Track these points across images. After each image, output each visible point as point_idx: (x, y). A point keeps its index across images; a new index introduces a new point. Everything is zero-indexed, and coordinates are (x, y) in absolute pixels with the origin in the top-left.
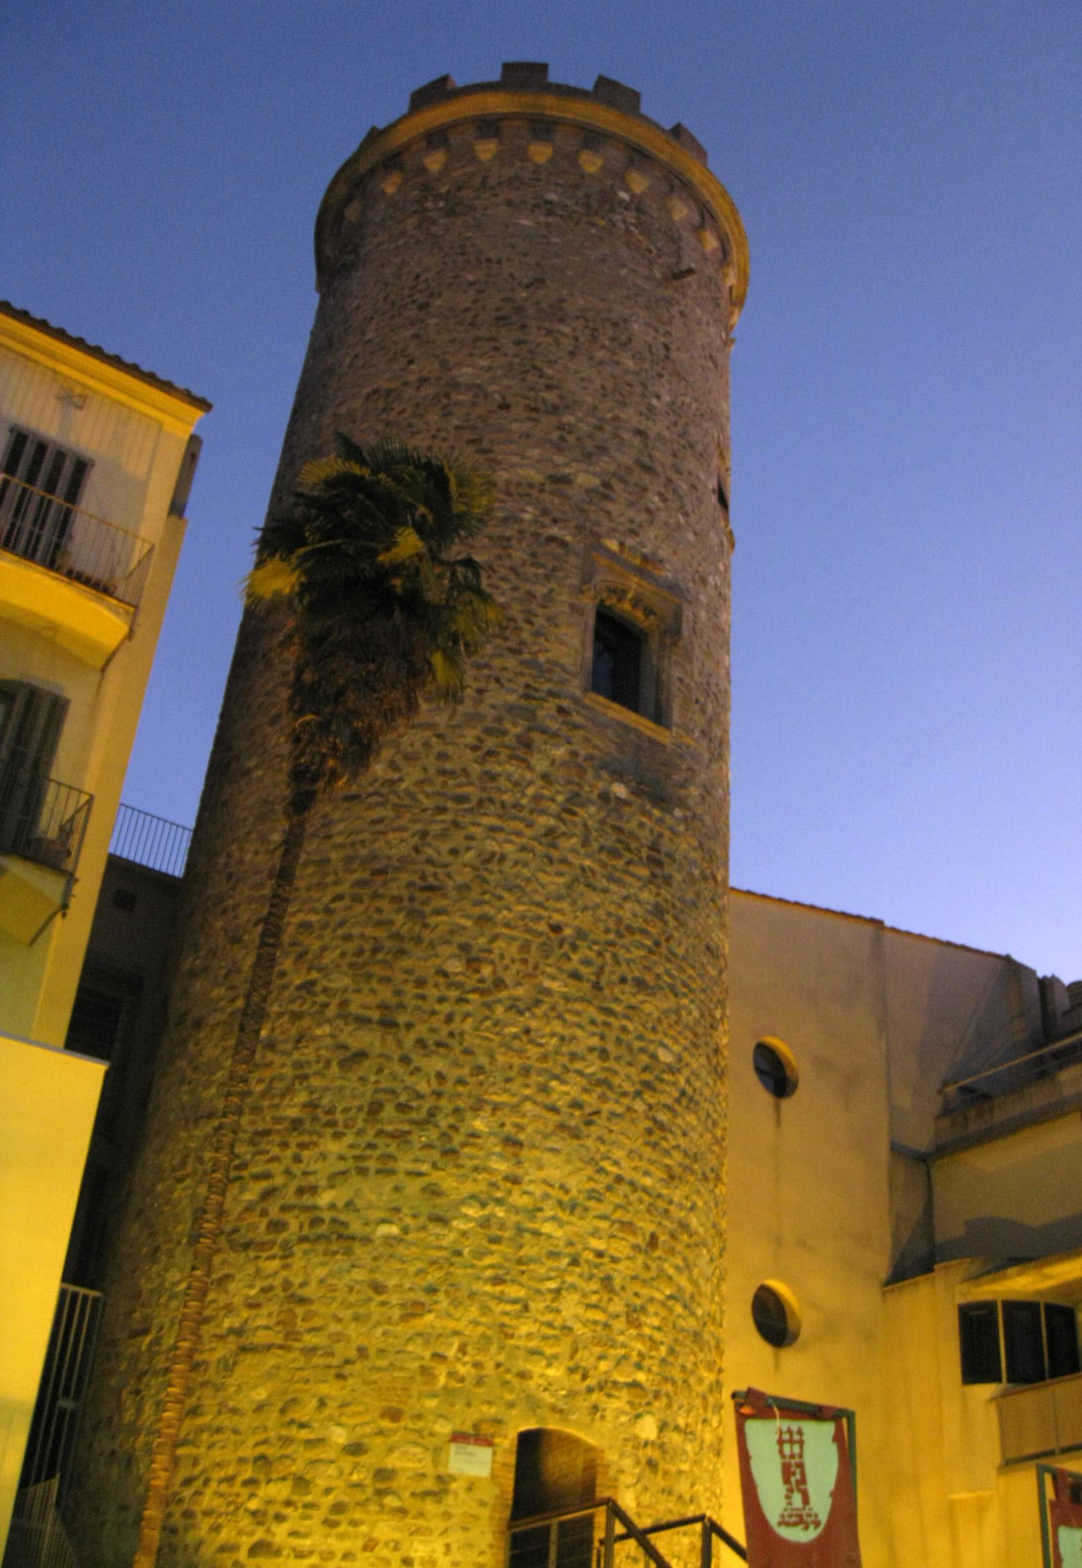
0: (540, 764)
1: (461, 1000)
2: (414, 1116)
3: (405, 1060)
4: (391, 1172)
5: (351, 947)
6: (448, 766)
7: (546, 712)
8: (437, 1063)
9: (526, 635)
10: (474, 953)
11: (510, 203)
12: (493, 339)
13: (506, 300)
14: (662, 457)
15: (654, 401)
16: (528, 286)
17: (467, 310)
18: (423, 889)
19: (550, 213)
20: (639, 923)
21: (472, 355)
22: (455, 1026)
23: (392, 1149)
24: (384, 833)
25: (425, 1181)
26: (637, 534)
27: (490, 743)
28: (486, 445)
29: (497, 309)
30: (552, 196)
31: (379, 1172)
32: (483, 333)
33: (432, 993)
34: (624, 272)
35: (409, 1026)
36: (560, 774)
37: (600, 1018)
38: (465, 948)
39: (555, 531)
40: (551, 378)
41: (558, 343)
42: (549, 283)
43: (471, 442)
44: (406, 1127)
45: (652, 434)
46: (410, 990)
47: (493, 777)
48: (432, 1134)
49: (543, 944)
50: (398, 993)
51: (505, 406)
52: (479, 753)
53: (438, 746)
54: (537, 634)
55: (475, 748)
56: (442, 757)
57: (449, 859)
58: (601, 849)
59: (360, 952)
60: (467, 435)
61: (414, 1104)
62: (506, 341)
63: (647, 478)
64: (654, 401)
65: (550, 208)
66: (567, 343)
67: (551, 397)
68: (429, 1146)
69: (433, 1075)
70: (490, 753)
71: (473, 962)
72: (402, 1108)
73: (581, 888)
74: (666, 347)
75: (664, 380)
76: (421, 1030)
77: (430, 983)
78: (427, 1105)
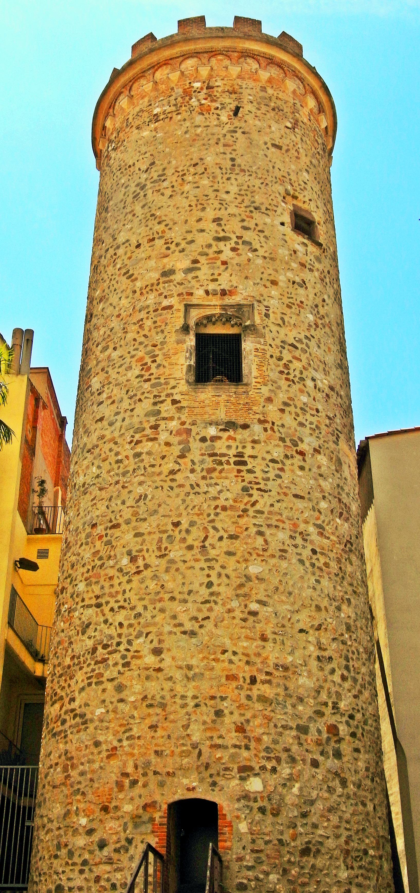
0: (163, 436)
1: (129, 581)
2: (110, 649)
3: (106, 622)
4: (102, 683)
5: (85, 570)
6: (120, 457)
7: (167, 408)
8: (120, 617)
9: (153, 370)
10: (134, 553)
11: (138, 128)
12: (132, 211)
13: (137, 185)
14: (233, 227)
15: (225, 196)
16: (146, 171)
17: (122, 201)
18: (111, 528)
19: (157, 121)
20: (227, 504)
21: (124, 225)
22: (127, 596)
23: (102, 671)
24: (95, 504)
25: (115, 683)
26: (217, 280)
27: (137, 437)
28: (131, 272)
29: (135, 192)
30: (156, 111)
31: (96, 683)
32: (129, 210)
33: (116, 582)
34: (199, 130)
35: (107, 603)
36: (174, 440)
37: (205, 565)
38: (129, 553)
39: (166, 303)
40: (160, 217)
41: (163, 194)
42: (157, 162)
43: (125, 274)
44: (107, 656)
45: (225, 218)
46: (107, 585)
47: (138, 455)
48: (117, 656)
49: (169, 537)
50: (102, 588)
51: (138, 246)
52: (133, 444)
53: (116, 448)
54: (159, 366)
55: (131, 442)
56: (117, 454)
57: (122, 507)
58: (202, 470)
59: (88, 571)
60: (124, 271)
61: (109, 643)
62: (138, 209)
63: (221, 244)
64: (225, 196)
65: (156, 118)
66: (168, 192)
67: (162, 227)
68: (116, 664)
69: (117, 624)
70: (138, 442)
71: (133, 560)
72: (105, 647)
73: (192, 496)
74: (233, 160)
75: (233, 181)
76: (112, 604)
77: (115, 577)
78: (114, 642)
